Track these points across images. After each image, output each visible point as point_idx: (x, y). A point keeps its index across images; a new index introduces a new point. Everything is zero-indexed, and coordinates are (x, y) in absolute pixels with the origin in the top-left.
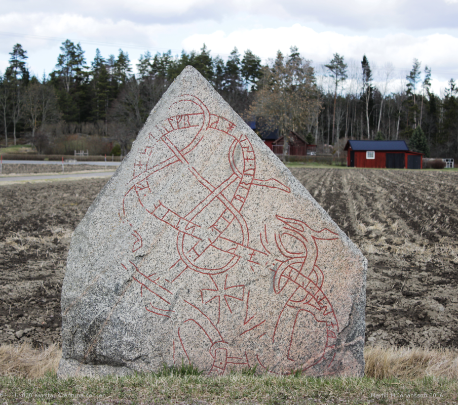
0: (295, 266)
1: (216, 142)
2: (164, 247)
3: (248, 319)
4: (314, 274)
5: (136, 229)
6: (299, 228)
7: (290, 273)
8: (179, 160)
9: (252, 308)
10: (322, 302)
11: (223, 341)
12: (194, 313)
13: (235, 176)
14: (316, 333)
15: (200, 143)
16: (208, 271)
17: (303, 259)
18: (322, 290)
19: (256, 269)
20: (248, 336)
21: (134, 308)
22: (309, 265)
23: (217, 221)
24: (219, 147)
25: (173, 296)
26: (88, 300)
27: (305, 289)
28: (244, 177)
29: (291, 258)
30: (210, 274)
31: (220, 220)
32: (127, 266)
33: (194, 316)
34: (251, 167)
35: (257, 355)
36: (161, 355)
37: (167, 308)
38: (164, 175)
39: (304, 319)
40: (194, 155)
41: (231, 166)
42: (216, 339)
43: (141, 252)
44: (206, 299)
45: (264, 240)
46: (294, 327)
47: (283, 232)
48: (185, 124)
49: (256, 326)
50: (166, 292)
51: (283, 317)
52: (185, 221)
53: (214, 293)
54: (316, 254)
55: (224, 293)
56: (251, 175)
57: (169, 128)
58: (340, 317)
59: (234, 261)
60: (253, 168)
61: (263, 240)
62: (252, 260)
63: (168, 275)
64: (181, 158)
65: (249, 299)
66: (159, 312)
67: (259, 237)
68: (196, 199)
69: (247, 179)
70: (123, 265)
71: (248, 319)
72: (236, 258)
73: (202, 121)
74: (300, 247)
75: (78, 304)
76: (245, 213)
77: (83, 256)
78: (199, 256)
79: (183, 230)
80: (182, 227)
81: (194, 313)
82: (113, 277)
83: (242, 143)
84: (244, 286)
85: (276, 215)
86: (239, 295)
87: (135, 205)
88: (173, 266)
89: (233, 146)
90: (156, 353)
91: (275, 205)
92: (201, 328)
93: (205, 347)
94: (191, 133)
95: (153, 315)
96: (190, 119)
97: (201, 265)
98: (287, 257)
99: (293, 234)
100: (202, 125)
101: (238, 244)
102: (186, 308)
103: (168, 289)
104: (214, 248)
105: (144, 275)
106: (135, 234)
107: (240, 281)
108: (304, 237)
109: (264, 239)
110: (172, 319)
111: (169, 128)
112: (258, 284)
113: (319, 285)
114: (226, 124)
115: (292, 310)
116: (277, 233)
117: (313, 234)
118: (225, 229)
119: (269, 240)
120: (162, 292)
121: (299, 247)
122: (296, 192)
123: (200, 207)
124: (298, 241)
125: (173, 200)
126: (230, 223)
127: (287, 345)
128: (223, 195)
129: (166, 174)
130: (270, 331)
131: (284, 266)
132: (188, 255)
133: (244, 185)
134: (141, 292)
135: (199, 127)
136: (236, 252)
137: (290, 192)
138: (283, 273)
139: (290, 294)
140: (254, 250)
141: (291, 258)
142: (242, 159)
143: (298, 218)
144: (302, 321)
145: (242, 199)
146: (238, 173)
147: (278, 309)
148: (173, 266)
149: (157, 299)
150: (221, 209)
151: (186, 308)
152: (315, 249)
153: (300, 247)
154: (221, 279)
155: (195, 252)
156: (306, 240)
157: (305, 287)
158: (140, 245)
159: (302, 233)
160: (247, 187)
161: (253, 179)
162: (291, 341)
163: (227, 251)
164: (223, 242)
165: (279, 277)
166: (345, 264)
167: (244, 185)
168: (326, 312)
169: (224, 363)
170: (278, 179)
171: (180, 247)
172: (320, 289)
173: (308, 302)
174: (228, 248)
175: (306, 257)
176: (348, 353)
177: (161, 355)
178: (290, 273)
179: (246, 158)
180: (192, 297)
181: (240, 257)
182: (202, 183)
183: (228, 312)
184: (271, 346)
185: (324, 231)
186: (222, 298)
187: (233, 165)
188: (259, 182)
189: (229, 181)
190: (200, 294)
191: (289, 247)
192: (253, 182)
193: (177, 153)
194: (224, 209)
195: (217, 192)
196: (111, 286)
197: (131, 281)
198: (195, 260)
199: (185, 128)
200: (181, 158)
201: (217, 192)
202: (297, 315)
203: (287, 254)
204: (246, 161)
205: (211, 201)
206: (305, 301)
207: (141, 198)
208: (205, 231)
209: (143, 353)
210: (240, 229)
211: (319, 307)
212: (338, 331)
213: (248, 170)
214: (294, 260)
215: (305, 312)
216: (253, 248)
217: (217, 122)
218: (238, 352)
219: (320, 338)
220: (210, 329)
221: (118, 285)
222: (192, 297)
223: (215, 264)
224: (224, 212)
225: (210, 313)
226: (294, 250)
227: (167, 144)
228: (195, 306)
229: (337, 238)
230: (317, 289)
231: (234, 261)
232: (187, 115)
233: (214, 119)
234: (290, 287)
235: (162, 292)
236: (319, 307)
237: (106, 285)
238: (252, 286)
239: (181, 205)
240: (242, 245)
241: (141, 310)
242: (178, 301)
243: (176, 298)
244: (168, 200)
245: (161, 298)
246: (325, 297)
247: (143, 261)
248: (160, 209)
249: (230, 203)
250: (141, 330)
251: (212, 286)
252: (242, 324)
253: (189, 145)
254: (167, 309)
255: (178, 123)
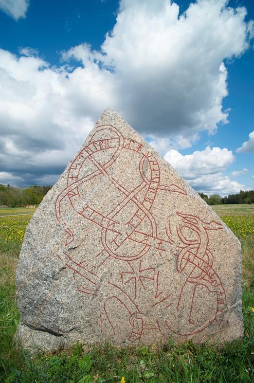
0: (193, 251)
1: (129, 158)
2: (91, 240)
3: (158, 294)
4: (206, 256)
5: (68, 227)
6: (194, 221)
7: (189, 256)
8: (102, 173)
9: (161, 285)
10: (213, 277)
11: (139, 313)
12: (116, 292)
13: (145, 183)
14: (209, 301)
15: (117, 160)
16: (126, 259)
17: (198, 245)
18: (213, 268)
19: (163, 255)
20: (159, 307)
21: (68, 289)
22: (203, 249)
23: (132, 218)
24: (132, 162)
25: (99, 279)
26: (33, 284)
27: (200, 268)
28: (152, 183)
29: (189, 245)
30: (128, 261)
31: (134, 218)
32: (61, 257)
33: (116, 294)
34: (157, 176)
35: (166, 322)
36: (91, 326)
37: (95, 288)
38: (90, 184)
39: (201, 291)
40: (113, 169)
41: (141, 176)
42: (134, 311)
43: (73, 245)
44: (125, 280)
45: (168, 232)
46: (193, 298)
47: (183, 225)
48: (105, 147)
49: (164, 299)
50: (93, 276)
51: (184, 291)
52: (106, 219)
53: (131, 276)
54: (207, 241)
55: (139, 275)
56: (157, 182)
57: (93, 149)
58: (226, 288)
59: (147, 249)
60: (158, 177)
61: (168, 233)
62: (160, 248)
63: (95, 262)
64: (103, 171)
65: (159, 279)
66: (88, 292)
67: (165, 230)
68: (115, 202)
69: (155, 185)
70: (58, 256)
71: (158, 294)
72: (148, 247)
73: (118, 144)
74: (196, 237)
75: (25, 286)
76: (153, 211)
77: (29, 248)
78: (119, 247)
79: (105, 226)
80: (105, 224)
81: (116, 292)
82: (50, 266)
83: (149, 158)
84: (154, 269)
85: (177, 213)
86: (151, 276)
87: (68, 208)
88: (98, 255)
89: (142, 160)
90: (87, 324)
91: (176, 205)
92: (122, 303)
93: (125, 318)
94: (110, 152)
95: (84, 294)
96: (109, 142)
97: (121, 254)
98: (186, 244)
99: (190, 226)
100: (118, 146)
101: (149, 236)
102: (110, 288)
103: (95, 273)
104: (130, 240)
105: (75, 263)
106: (68, 230)
107: (151, 265)
108: (198, 228)
109: (168, 231)
110: (99, 297)
111: (93, 149)
112: (165, 267)
113: (210, 265)
114: (137, 145)
115: (191, 285)
116: (178, 226)
117: (204, 226)
118: (139, 225)
119: (172, 232)
120: (90, 276)
121: (195, 236)
122: (190, 194)
123: (119, 208)
124: (194, 231)
125: (97, 203)
126: (142, 220)
127: (189, 312)
128: (136, 198)
129: (92, 184)
130: (175, 302)
131: (184, 251)
132: (110, 246)
133: (152, 190)
134: (74, 276)
135: (116, 148)
136: (148, 242)
137: (186, 194)
138: (183, 256)
139: (190, 273)
140: (161, 240)
141: (189, 245)
142: (149, 170)
143: (193, 214)
144: (199, 292)
145: (151, 201)
146: (147, 181)
147: (181, 285)
148: (98, 255)
149: (87, 281)
150: (135, 209)
151: (110, 288)
152: (206, 237)
153: (196, 237)
154: (136, 264)
155: (116, 244)
156: (200, 231)
157: (200, 266)
158: (72, 240)
159: (196, 225)
160: (154, 191)
161: (158, 185)
162: (191, 309)
163: (141, 242)
164: (137, 235)
165: (181, 260)
166: (228, 247)
167: (152, 190)
168: (216, 285)
169: (140, 330)
170: (177, 185)
171: (103, 240)
172: (211, 267)
173: (203, 278)
174: (141, 240)
175: (200, 244)
176: (233, 314)
177: (91, 326)
178: (189, 256)
179: (152, 169)
180: (114, 279)
181: (150, 246)
182: (119, 189)
183: (143, 290)
184: (176, 314)
185: (212, 223)
186: (137, 279)
187: (143, 175)
188: (164, 187)
189: (140, 187)
190: (120, 277)
191: (188, 236)
192: (159, 188)
193: (100, 168)
194: (137, 209)
195: (131, 196)
196: (49, 273)
197: (65, 268)
198: (115, 250)
199: (105, 149)
200: (103, 171)
201: (131, 196)
202: (195, 288)
203: (186, 242)
204: (153, 171)
205: (127, 203)
206: (200, 277)
207: (73, 202)
208: (123, 227)
209: (77, 325)
210: (150, 224)
211: (210, 281)
212: (225, 298)
213: (155, 178)
214: (191, 246)
215: (201, 286)
216: (161, 238)
217: (129, 144)
218: (152, 320)
219: (213, 304)
220: (129, 304)
221: (54, 272)
222: (114, 279)
223: (131, 252)
224: (137, 212)
225: (129, 291)
226: (191, 239)
227: (92, 161)
228: (116, 286)
229: (222, 228)
230: (209, 267)
231: (147, 249)
232: (107, 140)
233: (127, 142)
234: (189, 267)
235: (90, 276)
236: (210, 281)
237: (45, 273)
238: (160, 268)
239: (103, 207)
240: (152, 237)
241: (74, 291)
242: (103, 283)
243: (102, 280)
244: (93, 204)
245: (90, 281)
246: (215, 273)
247: (74, 252)
248: (87, 210)
249: (142, 204)
250: (74, 307)
251: (130, 270)
252: (154, 298)
253: (108, 162)
254: (95, 289)
255: (100, 145)
